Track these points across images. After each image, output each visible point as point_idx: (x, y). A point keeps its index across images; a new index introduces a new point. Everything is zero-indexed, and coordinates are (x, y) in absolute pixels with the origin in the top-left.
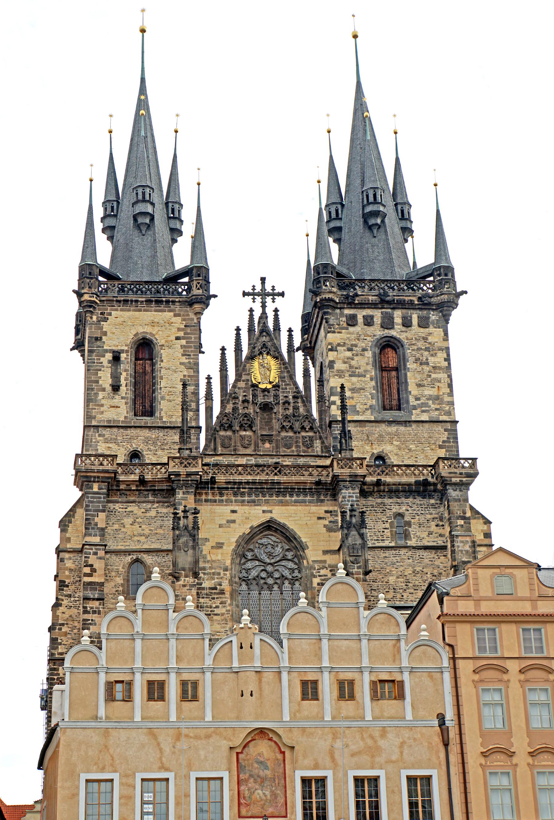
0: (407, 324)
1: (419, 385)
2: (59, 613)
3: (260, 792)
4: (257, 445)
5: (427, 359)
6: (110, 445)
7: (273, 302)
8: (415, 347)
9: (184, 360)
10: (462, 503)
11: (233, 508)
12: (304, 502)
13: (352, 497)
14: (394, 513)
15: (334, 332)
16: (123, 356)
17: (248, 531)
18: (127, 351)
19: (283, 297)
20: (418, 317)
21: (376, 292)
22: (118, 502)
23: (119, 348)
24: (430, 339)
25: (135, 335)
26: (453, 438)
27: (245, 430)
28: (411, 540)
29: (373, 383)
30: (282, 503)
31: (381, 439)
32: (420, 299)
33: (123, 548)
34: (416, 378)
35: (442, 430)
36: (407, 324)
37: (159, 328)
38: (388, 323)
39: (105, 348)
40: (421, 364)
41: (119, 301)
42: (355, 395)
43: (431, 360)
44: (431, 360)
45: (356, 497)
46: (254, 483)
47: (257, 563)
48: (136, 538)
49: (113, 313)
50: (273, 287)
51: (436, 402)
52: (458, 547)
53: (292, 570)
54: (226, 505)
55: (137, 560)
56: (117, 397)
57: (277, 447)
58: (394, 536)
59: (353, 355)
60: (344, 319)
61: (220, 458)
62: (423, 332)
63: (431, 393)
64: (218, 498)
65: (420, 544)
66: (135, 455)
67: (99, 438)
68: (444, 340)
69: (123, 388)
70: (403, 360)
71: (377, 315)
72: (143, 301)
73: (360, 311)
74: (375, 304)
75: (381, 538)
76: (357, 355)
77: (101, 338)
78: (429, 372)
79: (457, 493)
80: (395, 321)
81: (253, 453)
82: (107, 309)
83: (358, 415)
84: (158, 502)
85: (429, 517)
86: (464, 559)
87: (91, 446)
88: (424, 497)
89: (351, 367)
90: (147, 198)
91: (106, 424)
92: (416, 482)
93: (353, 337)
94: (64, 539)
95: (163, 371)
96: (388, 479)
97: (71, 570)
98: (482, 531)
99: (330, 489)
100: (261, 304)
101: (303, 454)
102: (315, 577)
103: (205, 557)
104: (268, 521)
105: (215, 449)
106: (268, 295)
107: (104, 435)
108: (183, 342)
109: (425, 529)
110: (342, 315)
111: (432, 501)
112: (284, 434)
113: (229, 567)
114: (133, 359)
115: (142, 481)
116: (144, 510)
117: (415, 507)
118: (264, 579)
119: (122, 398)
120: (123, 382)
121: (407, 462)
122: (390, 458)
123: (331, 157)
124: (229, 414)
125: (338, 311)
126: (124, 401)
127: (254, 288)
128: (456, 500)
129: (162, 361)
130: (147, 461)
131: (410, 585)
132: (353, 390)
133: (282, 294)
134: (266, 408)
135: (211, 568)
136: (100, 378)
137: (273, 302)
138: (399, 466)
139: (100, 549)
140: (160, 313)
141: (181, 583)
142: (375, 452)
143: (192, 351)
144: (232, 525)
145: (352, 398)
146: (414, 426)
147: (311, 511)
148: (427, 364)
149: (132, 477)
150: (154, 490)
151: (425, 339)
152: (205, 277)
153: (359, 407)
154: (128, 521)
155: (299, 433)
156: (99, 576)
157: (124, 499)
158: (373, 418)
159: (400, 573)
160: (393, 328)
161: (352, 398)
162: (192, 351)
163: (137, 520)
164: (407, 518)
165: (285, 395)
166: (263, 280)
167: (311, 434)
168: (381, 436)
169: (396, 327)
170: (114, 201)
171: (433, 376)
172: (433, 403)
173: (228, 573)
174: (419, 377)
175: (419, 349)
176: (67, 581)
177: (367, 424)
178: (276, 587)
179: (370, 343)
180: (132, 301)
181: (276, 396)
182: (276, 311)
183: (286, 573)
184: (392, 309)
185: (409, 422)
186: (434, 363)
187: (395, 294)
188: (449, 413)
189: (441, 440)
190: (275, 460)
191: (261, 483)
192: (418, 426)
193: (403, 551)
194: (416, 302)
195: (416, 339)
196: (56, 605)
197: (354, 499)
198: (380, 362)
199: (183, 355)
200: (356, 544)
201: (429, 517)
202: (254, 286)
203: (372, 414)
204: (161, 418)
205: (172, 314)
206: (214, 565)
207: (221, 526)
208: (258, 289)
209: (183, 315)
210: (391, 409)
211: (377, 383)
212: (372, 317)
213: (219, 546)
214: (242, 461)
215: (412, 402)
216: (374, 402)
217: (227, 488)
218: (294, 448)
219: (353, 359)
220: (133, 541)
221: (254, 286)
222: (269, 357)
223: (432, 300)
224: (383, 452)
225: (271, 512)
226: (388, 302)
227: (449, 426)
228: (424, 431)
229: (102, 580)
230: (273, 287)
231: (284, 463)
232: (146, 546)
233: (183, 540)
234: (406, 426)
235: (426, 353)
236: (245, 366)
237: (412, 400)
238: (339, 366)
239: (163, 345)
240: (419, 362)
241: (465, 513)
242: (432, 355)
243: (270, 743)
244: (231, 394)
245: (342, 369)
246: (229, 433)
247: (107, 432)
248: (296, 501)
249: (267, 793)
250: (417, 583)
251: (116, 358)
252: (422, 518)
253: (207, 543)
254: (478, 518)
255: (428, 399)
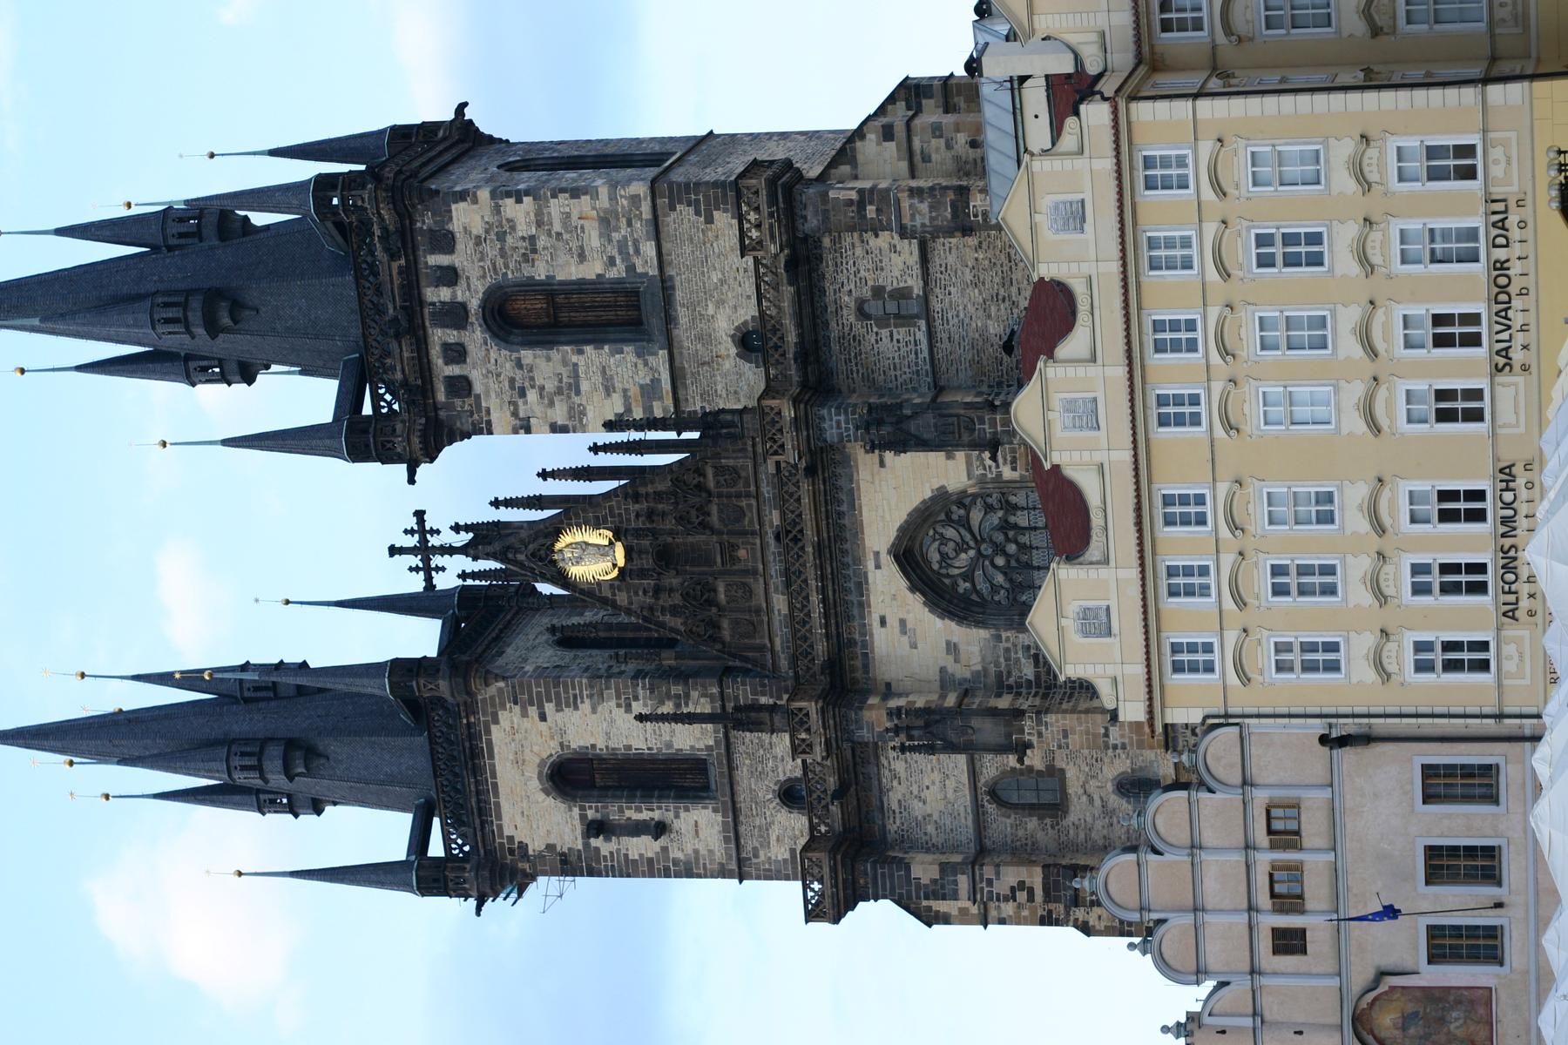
0: (450, 276)
1: (582, 257)
2: (1101, 926)
3: (1452, 1027)
4: (746, 572)
5: (523, 238)
6: (773, 838)
7: (438, 532)
8: (500, 262)
9: (586, 706)
10: (830, 207)
11: (876, 623)
12: (851, 492)
13: (838, 422)
14: (858, 319)
15: (489, 423)
16: (591, 814)
17: (919, 598)
18: (582, 808)
19: (424, 512)
20: (432, 253)
21: (394, 345)
22: (884, 826)
23: (577, 822)
24: (478, 229)
25: (548, 794)
26: (688, 193)
27: (715, 591)
28: (910, 289)
29: (589, 349)
30: (858, 530)
31: (706, 338)
32: (393, 257)
33: (970, 818)
34: (568, 263)
35: (673, 215)
36: (450, 276)
37: (527, 751)
38: (455, 315)
39: (580, 847)
40: (534, 251)
41: (483, 823)
42: (618, 386)
43: (524, 229)
44: (524, 229)
45: (838, 414)
46: (823, 591)
47: (979, 573)
48: (950, 795)
49: (507, 833)
50: (406, 532)
51: (613, 223)
52: (923, 225)
53: (989, 508)
54: (872, 635)
55: (993, 794)
56: (677, 824)
57: (744, 533)
58: (903, 319)
59: (533, 387)
60: (458, 402)
61: (778, 641)
62: (463, 246)
63: (595, 234)
64: (859, 650)
65: (917, 270)
66: (789, 795)
67: (762, 857)
68: (475, 201)
69: (656, 815)
70: (530, 287)
71: (439, 336)
72: (477, 782)
73: (435, 372)
74: (418, 340)
75: (912, 346)
76: (532, 379)
77: (563, 854)
78: (550, 235)
79: (809, 213)
80: (447, 299)
81: (761, 580)
82: (502, 844)
83: (659, 380)
84: (877, 757)
85: (859, 251)
86: (948, 213)
87: (779, 871)
88: (820, 259)
89: (559, 391)
90: (252, 761)
91: (733, 846)
92: (790, 284)
93: (494, 386)
94: (964, 918)
95: (611, 745)
96: (792, 338)
97: (1020, 906)
98: (878, 144)
99: (825, 467)
100: (447, 557)
101: (753, 488)
102: (999, 475)
103: (976, 674)
104: (897, 558)
105: (761, 648)
106: (423, 540)
107: (755, 849)
108: (549, 708)
109: (885, 260)
110: (449, 406)
111: (826, 241)
112: (714, 519)
113: (993, 631)
114: (595, 793)
115: (839, 794)
116: (895, 783)
117: (842, 278)
118: (1008, 562)
119: (677, 816)
120: (645, 815)
121: (749, 287)
122: (745, 323)
123: (80, 368)
124: (684, 624)
125: (442, 414)
126: (683, 814)
127: (416, 569)
128: (826, 219)
129: (593, 746)
130: (798, 773)
131: (1002, 292)
132: (609, 390)
133: (420, 515)
134: (666, 557)
135: (997, 664)
136: (641, 855)
137: (438, 532)
138: (762, 313)
139: (981, 875)
140: (496, 751)
141: (1034, 739)
142: (733, 351)
143: (566, 692)
144: (909, 626)
145: (625, 391)
146: (671, 272)
147: (869, 478)
148: (532, 239)
149: (835, 809)
150: (855, 764)
151: (478, 241)
152: (410, 670)
153: (644, 377)
154: (918, 809)
155: (710, 493)
156: (1031, 876)
157: (877, 814)
158: (663, 353)
159: (981, 313)
160: (463, 306)
161: (625, 391)
162: (566, 692)
163: (915, 792)
164: (867, 293)
165: (633, 516)
166: (394, 551)
167: (710, 472)
168: (699, 338)
169: (460, 299)
170: (258, 800)
171: (557, 227)
172: (617, 229)
173: (1004, 635)
174: (562, 258)
175: (502, 251)
176: (1040, 912)
177: (677, 363)
178: (1024, 539)
179: (504, 352)
180: (479, 801)
181: (638, 533)
182: (457, 528)
183: (995, 518)
184: (422, 308)
185: (663, 281)
186: (528, 224)
187: (390, 306)
188: (635, 200)
189: (694, 218)
190: (772, 542)
191: (823, 578)
192: (670, 263)
193: (936, 305)
194: (403, 262)
195: (481, 260)
196: (1087, 930)
197: (842, 418)
198: (538, 327)
199: (576, 708)
200: (936, 425)
201: (859, 251)
202: (411, 569)
203: (656, 354)
204: (709, 748)
205: (494, 728)
206: (989, 659)
207: (914, 646)
208: (415, 561)
209: (493, 705)
210: (638, 308)
211: (588, 342)
212: (446, 347)
213: (952, 648)
214: (780, 603)
215: (617, 272)
216: (628, 349)
217: (838, 635)
218: (744, 503)
219: (542, 388)
220: (956, 799)
221: (411, 569)
222: (558, 546)
223: (391, 228)
224: (733, 336)
225: (877, 554)
226: (411, 320)
227: (663, 202)
228: (681, 255)
229: (1039, 870)
230: (406, 532)
231: (776, 522)
232: (965, 778)
233: (952, 736)
234: (673, 288)
235: (509, 239)
236: (582, 591)
237: (613, 274)
238: (559, 414)
239: (561, 744)
240: (531, 256)
241: (850, 202)
242: (513, 228)
243: (1376, 1007)
244: (645, 619)
245: (565, 409)
246: (725, 624)
247: (749, 844)
248: (852, 505)
249: (1454, 1014)
250: (997, 280)
251: (597, 828)
252: (864, 264)
253: (950, 670)
254: (854, 150)
255: (610, 241)
